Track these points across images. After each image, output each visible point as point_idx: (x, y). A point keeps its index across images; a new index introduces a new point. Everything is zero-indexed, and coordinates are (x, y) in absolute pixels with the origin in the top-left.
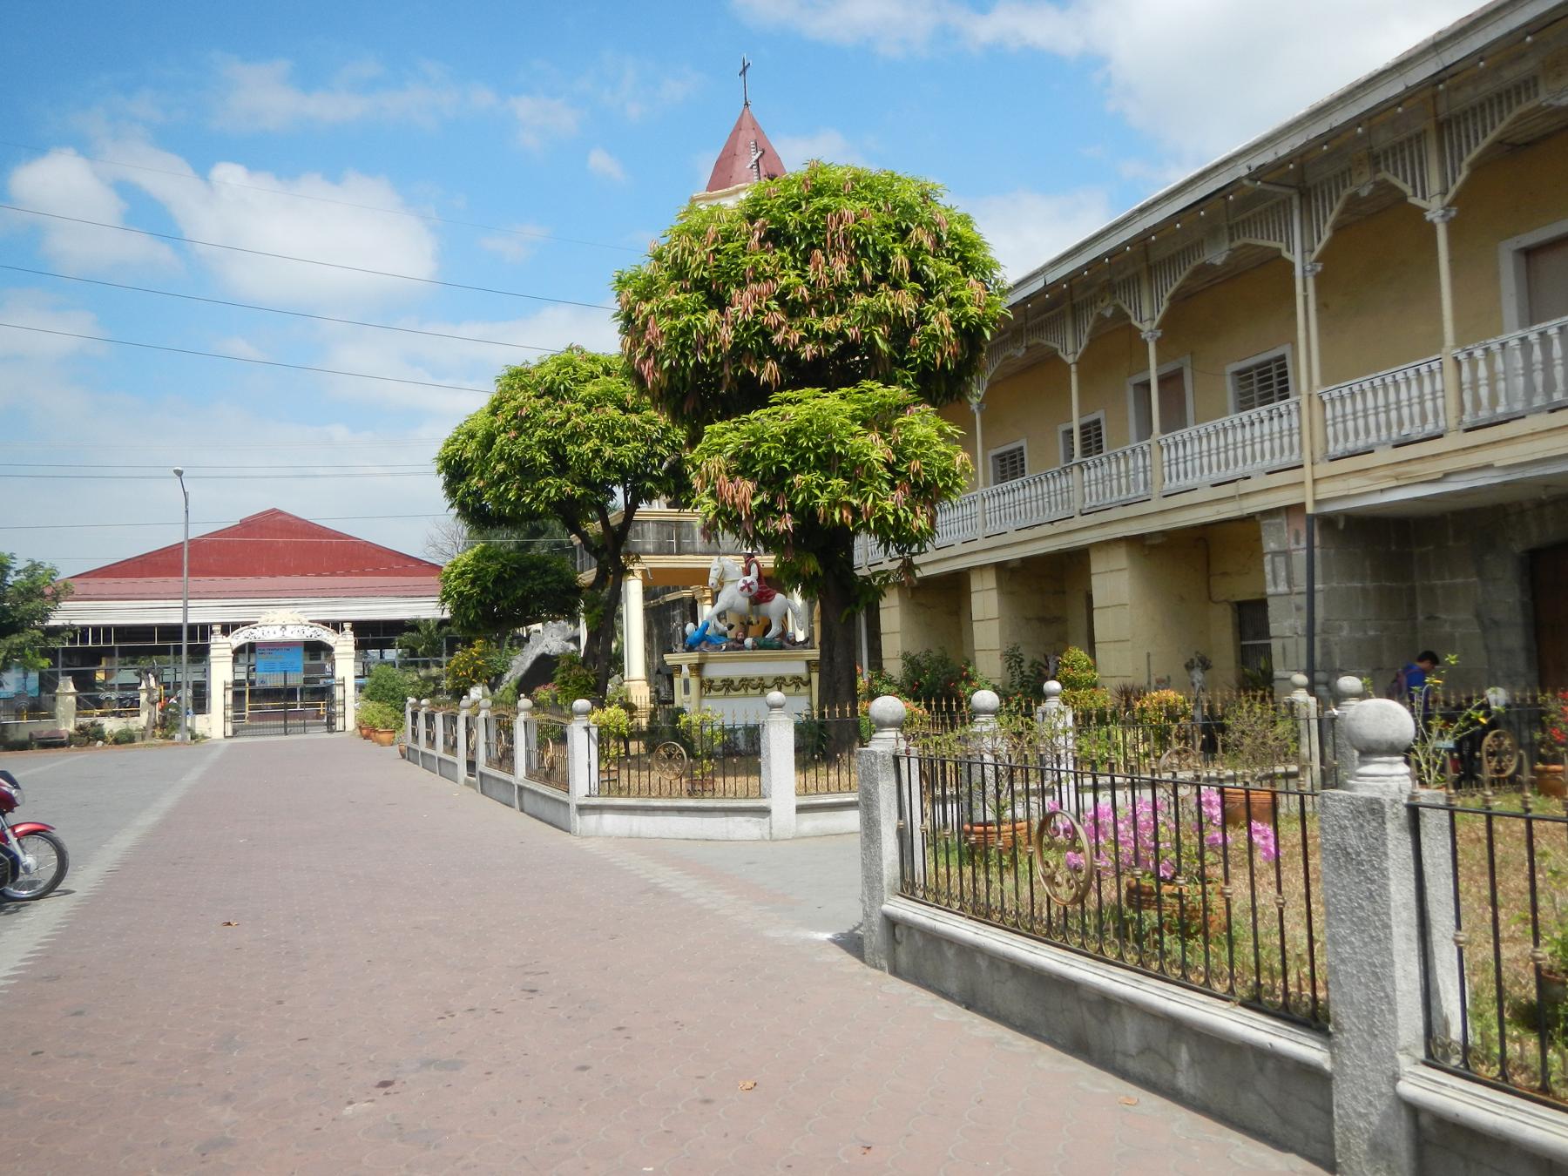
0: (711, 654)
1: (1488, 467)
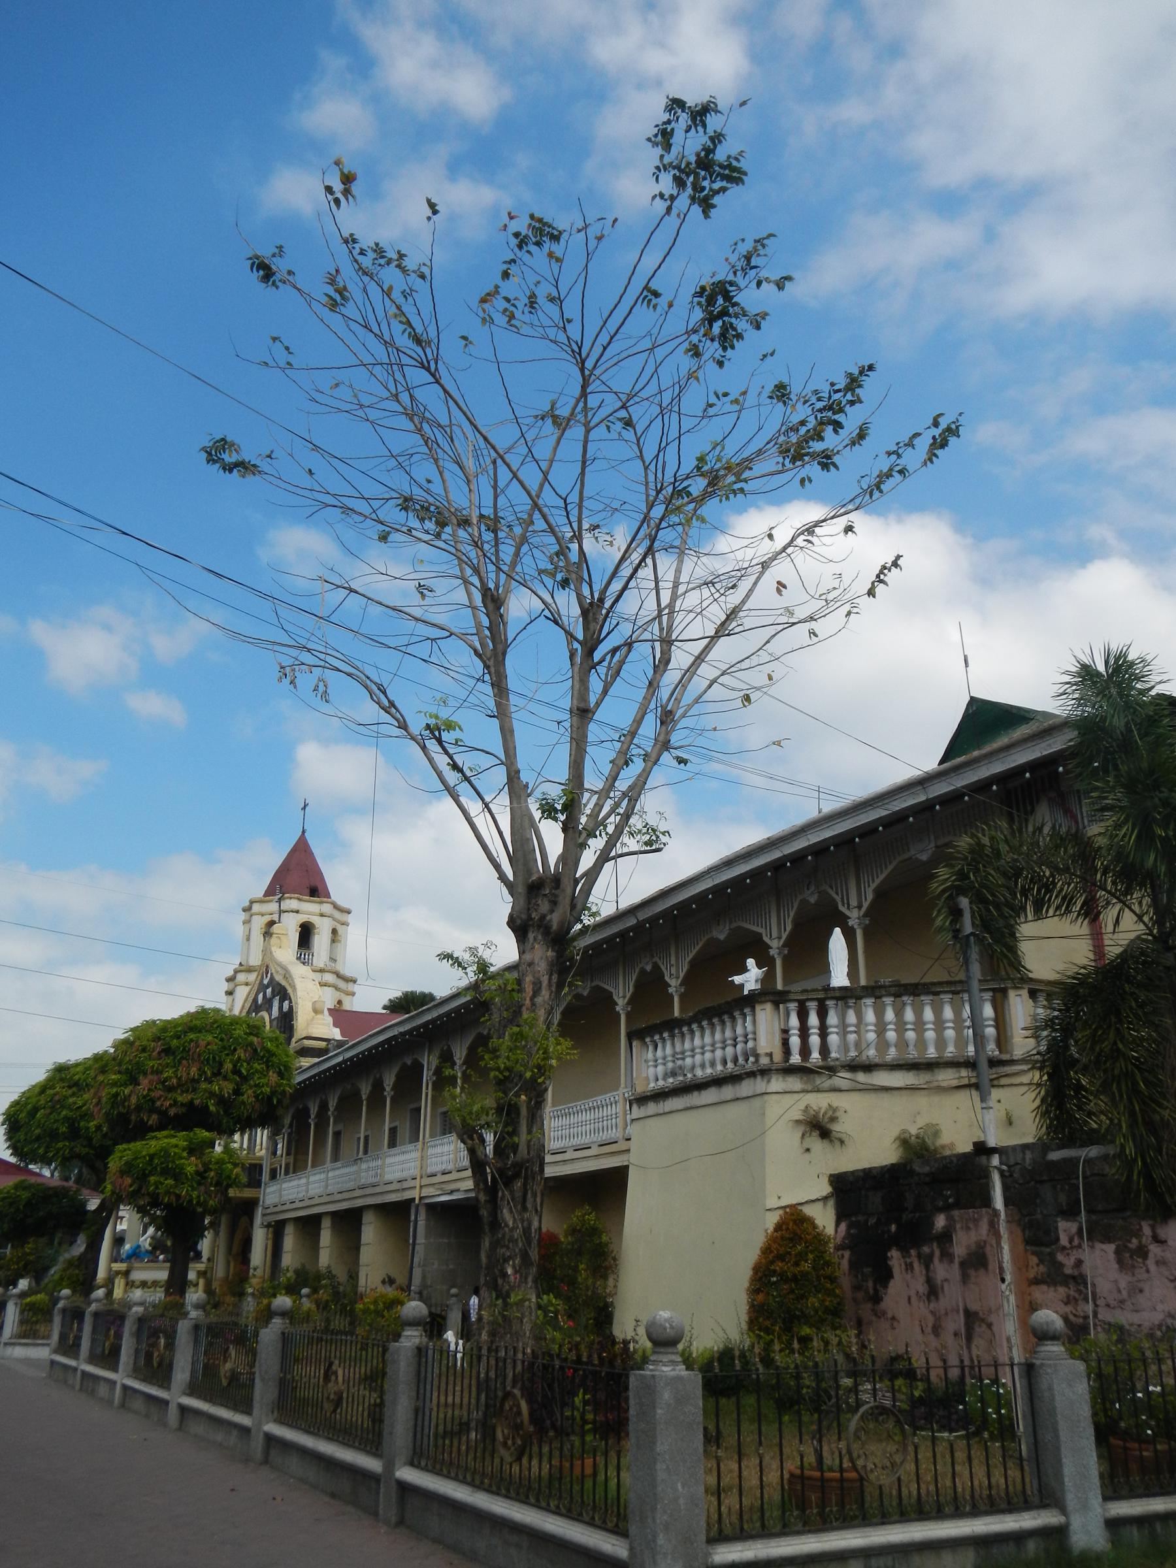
0: (136, 1265)
1: (458, 1190)
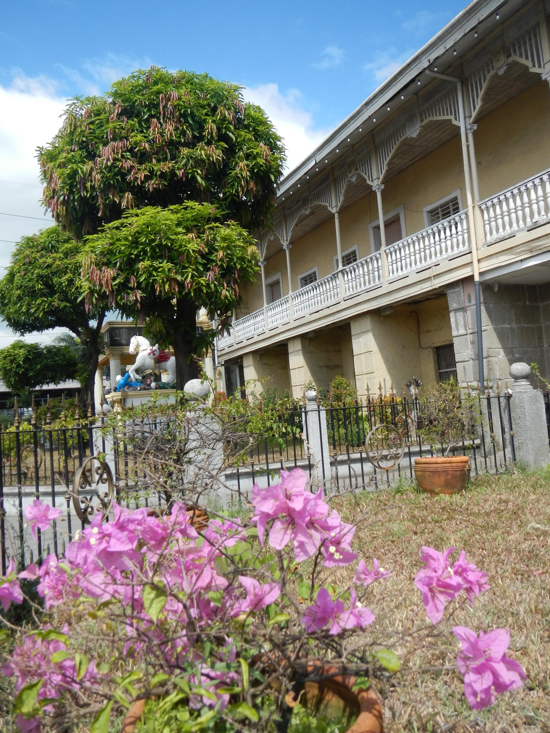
0: (130, 393)
